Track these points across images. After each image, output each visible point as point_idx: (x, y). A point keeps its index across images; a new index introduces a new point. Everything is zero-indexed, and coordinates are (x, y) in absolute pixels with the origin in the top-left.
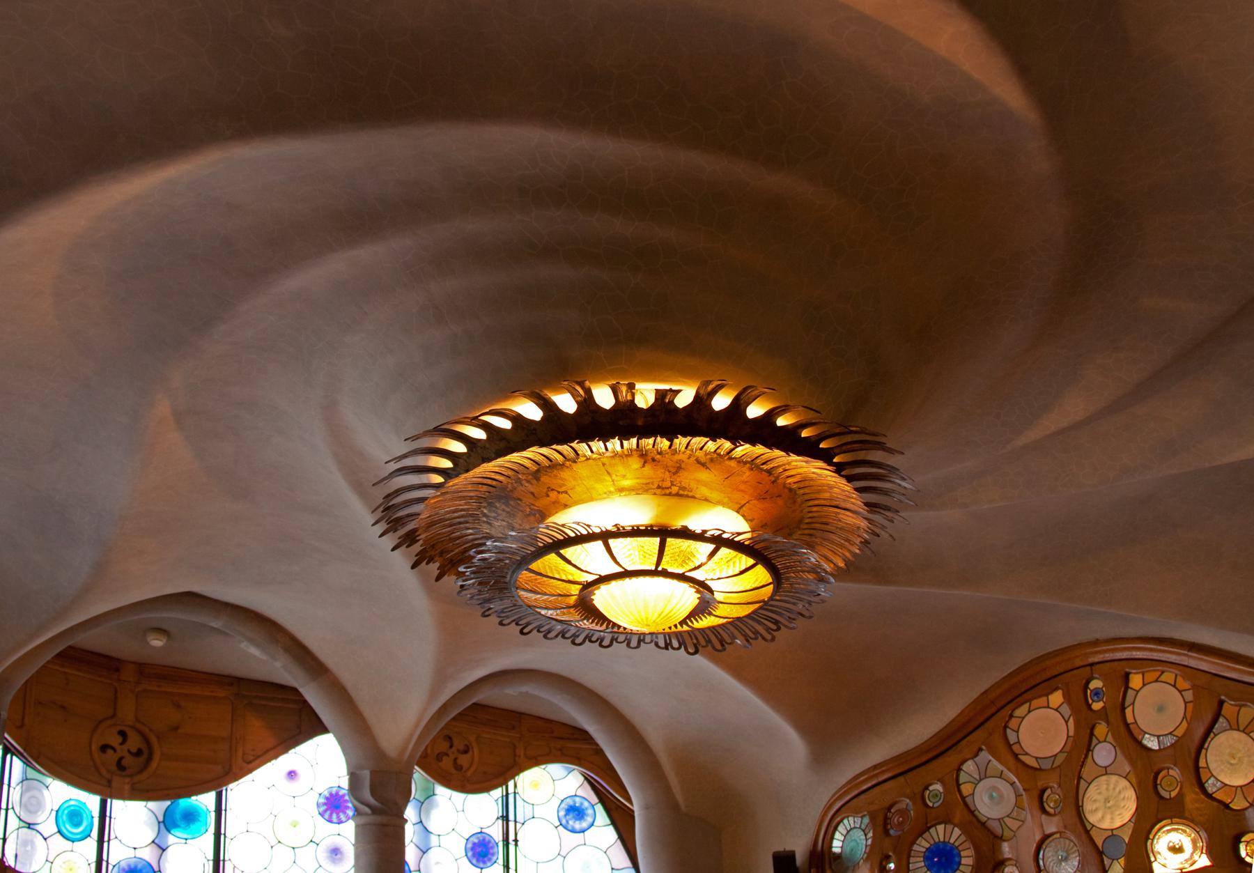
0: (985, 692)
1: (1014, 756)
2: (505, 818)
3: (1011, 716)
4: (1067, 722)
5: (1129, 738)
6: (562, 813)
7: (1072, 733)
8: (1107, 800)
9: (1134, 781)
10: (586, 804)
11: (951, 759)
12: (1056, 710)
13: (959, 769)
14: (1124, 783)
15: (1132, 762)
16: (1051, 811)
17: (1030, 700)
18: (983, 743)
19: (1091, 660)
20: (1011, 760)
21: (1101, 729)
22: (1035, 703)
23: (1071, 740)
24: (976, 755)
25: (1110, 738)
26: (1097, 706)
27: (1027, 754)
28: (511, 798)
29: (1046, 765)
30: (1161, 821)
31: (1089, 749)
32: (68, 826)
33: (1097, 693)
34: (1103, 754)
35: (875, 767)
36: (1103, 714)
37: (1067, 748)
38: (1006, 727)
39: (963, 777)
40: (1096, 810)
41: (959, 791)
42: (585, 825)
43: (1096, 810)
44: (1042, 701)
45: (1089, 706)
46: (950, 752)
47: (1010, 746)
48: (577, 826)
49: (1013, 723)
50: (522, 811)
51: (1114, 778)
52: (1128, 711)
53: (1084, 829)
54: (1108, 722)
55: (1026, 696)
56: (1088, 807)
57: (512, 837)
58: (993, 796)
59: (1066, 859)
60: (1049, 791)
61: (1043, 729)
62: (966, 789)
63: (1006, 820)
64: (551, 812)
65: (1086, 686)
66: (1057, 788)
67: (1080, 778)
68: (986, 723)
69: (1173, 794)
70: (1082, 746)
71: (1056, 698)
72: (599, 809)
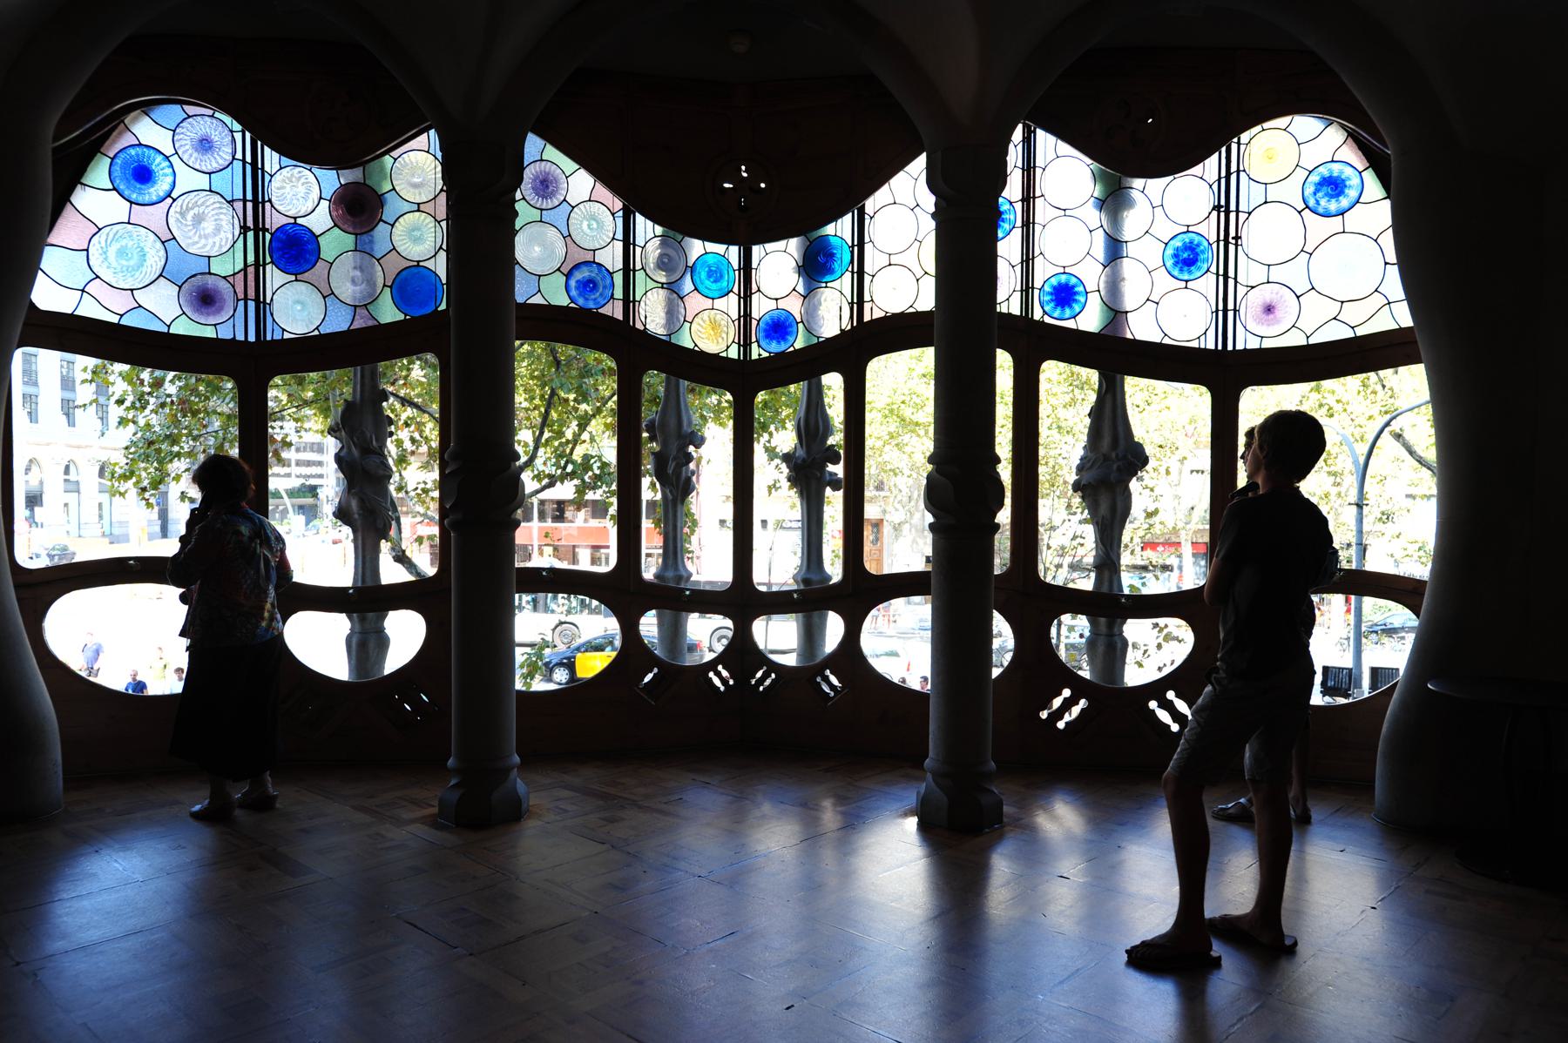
2: (1222, 208)
6: (1310, 190)
10: (1348, 171)
28: (1233, 178)
32: (708, 283)
42: (1344, 202)
48: (1333, 206)
50: (1249, 194)
57: (1232, 233)
64: (1291, 192)
72: (1370, 178)
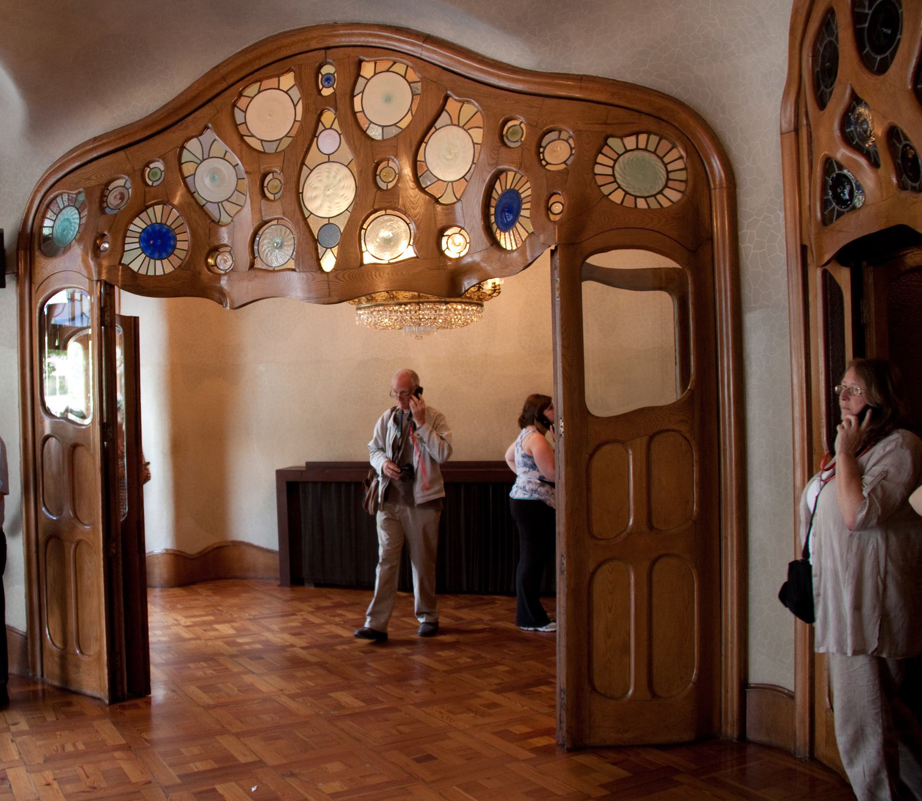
0: (217, 67)
1: (238, 137)
3: (241, 95)
4: (295, 106)
5: (354, 128)
7: (299, 118)
8: (327, 188)
9: (355, 170)
11: (174, 136)
12: (286, 92)
13: (183, 147)
14: (346, 171)
15: (355, 150)
16: (271, 197)
17: (260, 81)
18: (210, 121)
20: (236, 139)
21: (328, 117)
22: (267, 83)
23: (297, 124)
24: (201, 134)
25: (336, 126)
26: (327, 92)
27: (252, 136)
29: (270, 148)
30: (375, 211)
31: (315, 135)
33: (328, 79)
34: (328, 141)
35: (95, 139)
36: (332, 102)
37: (293, 133)
38: (234, 105)
39: (186, 156)
40: (315, 197)
41: (181, 170)
43: (315, 197)
44: (273, 82)
45: (319, 91)
46: (173, 129)
47: (237, 126)
49: (242, 103)
51: (336, 166)
52: (357, 100)
53: (301, 215)
54: (336, 110)
55: (257, 75)
56: (308, 194)
58: (214, 175)
59: (281, 246)
60: (270, 177)
61: (271, 111)
62: (187, 169)
63: (226, 204)
65: (318, 71)
66: (278, 173)
67: (303, 163)
69: (390, 186)
70: (308, 133)
71: (288, 80)
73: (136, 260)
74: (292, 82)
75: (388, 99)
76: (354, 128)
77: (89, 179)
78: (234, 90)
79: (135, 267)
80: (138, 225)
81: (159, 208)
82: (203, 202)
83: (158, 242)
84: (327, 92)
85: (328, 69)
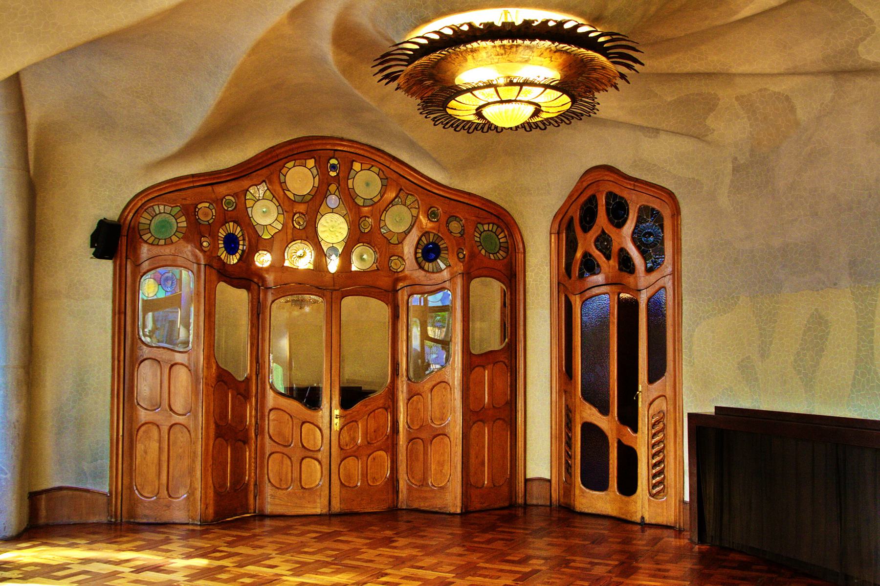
7: (316, 185)
14: (343, 220)
18: (267, 178)
19: (336, 148)
21: (333, 188)
25: (337, 193)
26: (333, 174)
33: (333, 167)
34: (333, 200)
35: (193, 176)
49: (284, 171)
52: (350, 182)
56: (320, 229)
61: (300, 179)
68: (267, 166)
69: (366, 231)
71: (311, 163)
73: (223, 255)
74: (313, 164)
75: (367, 184)
76: (349, 198)
77: (185, 199)
78: (281, 163)
79: (223, 257)
80: (222, 234)
81: (231, 224)
82: (255, 224)
83: (231, 244)
84: (333, 174)
85: (333, 161)
